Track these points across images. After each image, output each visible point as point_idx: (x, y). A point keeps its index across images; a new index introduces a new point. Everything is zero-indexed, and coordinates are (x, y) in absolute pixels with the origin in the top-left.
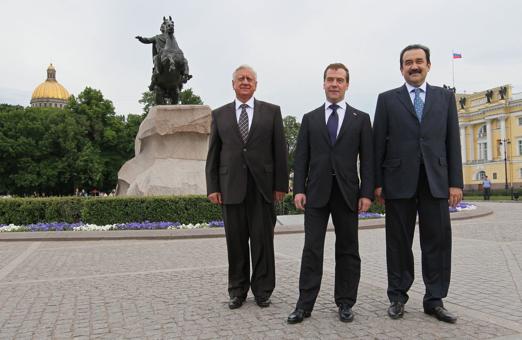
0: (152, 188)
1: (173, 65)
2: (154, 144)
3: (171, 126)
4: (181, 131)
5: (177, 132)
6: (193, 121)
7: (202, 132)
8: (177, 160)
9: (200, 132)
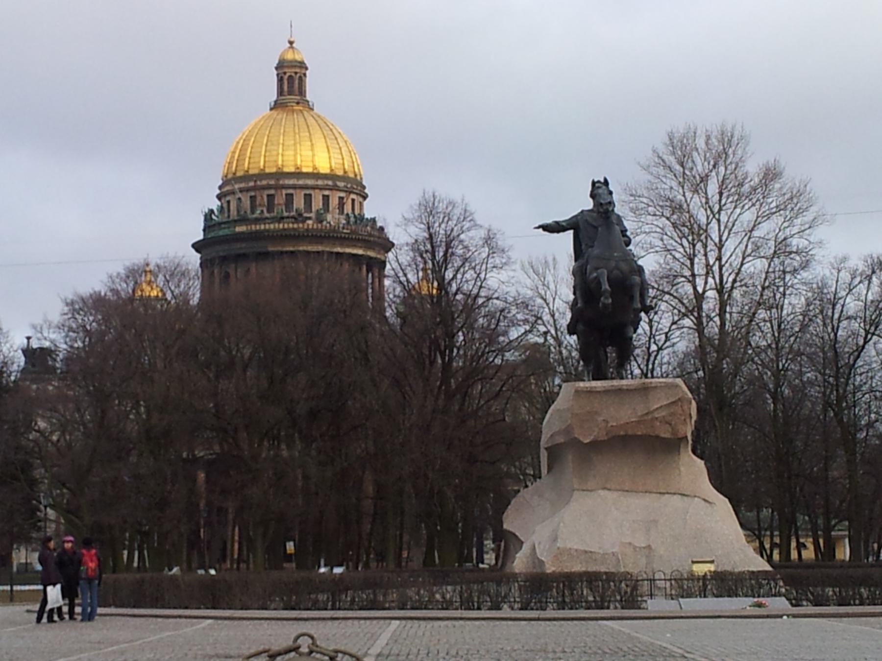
0: (561, 553)
1: (607, 295)
2: (570, 459)
3: (604, 424)
4: (622, 433)
5: (614, 437)
6: (647, 414)
7: (667, 435)
8: (615, 494)
9: (663, 435)
